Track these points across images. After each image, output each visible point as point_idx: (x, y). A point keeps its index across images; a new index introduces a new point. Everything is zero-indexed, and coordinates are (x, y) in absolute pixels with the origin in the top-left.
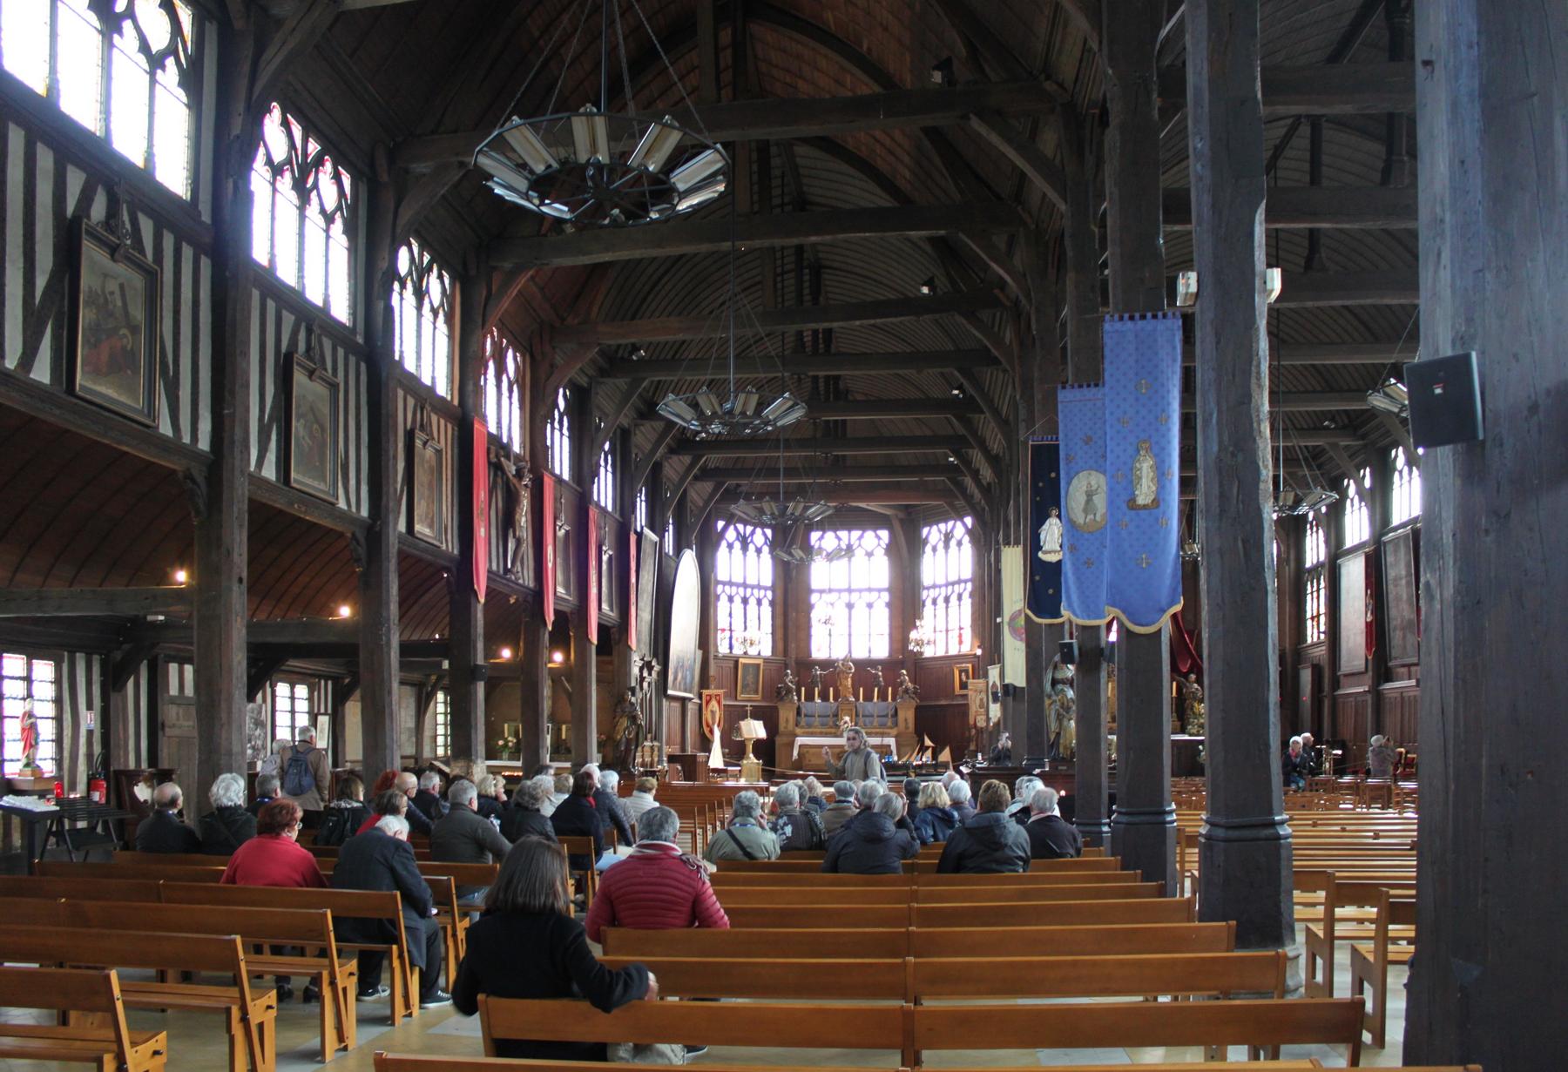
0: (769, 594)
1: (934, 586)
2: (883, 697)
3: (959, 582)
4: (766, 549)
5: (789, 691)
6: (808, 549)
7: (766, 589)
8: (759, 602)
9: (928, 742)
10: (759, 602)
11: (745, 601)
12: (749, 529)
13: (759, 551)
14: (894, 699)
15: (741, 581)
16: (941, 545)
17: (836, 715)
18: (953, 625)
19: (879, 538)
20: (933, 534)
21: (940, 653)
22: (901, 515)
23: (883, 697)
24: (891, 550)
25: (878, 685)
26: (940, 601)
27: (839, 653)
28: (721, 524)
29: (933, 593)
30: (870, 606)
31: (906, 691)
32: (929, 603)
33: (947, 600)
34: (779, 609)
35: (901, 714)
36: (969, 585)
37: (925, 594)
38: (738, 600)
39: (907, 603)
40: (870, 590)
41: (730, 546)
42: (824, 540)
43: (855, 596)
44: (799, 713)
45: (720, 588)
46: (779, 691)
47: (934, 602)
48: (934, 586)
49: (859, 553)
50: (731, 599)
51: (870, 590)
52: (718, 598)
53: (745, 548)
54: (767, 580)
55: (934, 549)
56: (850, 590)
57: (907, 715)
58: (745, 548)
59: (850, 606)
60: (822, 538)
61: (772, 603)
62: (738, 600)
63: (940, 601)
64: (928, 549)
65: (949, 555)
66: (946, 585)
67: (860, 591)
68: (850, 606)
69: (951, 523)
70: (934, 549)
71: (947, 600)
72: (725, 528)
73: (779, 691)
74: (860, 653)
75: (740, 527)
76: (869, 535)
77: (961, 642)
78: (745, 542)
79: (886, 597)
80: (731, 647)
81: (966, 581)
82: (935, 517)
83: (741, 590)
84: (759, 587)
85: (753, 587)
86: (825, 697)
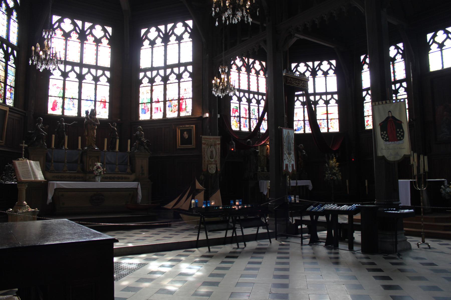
2: (123, 148)
3: (179, 65)
9: (198, 186)
17: (82, 161)
19: (105, 31)
21: (158, 116)
23: (123, 148)
26: (158, 80)
27: (71, 112)
29: (149, 74)
30: (96, 79)
31: (141, 143)
32: (145, 81)
36: (190, 68)
37: (142, 75)
39: (125, 79)
40: (97, 67)
47: (152, 81)
48: (152, 69)
49: (90, 39)
55: (152, 43)
56: (81, 65)
57: (142, 163)
59: (81, 77)
60: (60, 21)
63: (158, 80)
64: (146, 43)
68: (81, 77)
69: (170, 26)
70: (152, 43)
71: (165, 79)
77: (180, 109)
79: (108, 74)
81: (186, 65)
86: (73, 145)
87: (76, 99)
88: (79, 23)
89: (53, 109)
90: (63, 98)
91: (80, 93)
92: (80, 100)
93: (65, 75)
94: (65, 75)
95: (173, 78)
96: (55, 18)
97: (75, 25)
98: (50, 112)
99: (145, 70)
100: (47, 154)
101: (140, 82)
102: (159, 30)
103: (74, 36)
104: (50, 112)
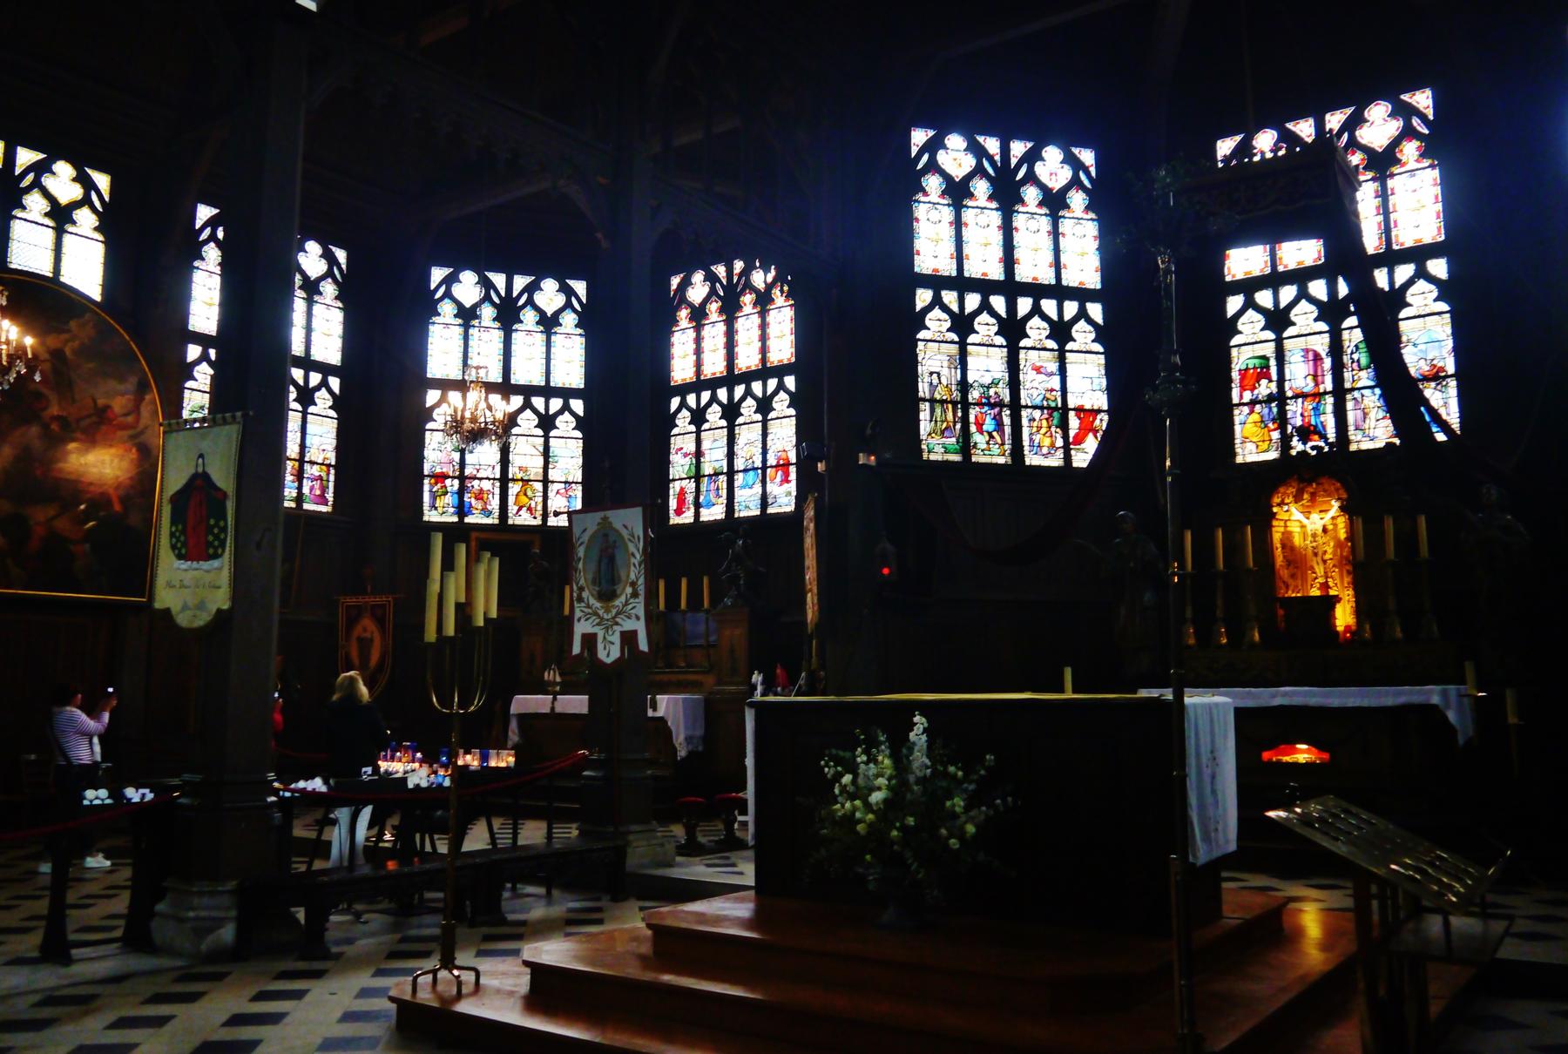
0: (1095, 311)
8: (1061, 332)
10: (1061, 332)
11: (1012, 330)
12: (1018, 148)
28: (919, 137)
38: (985, 327)
41: (957, 192)
45: (923, 297)
50: (962, 325)
52: (918, 321)
61: (1102, 334)
62: (985, 327)
72: (933, 146)
75: (992, 145)
80: (966, 446)
83: (998, 303)
84: (1060, 292)
85: (1037, 291)
87: (1326, 393)
92: (1340, 393)
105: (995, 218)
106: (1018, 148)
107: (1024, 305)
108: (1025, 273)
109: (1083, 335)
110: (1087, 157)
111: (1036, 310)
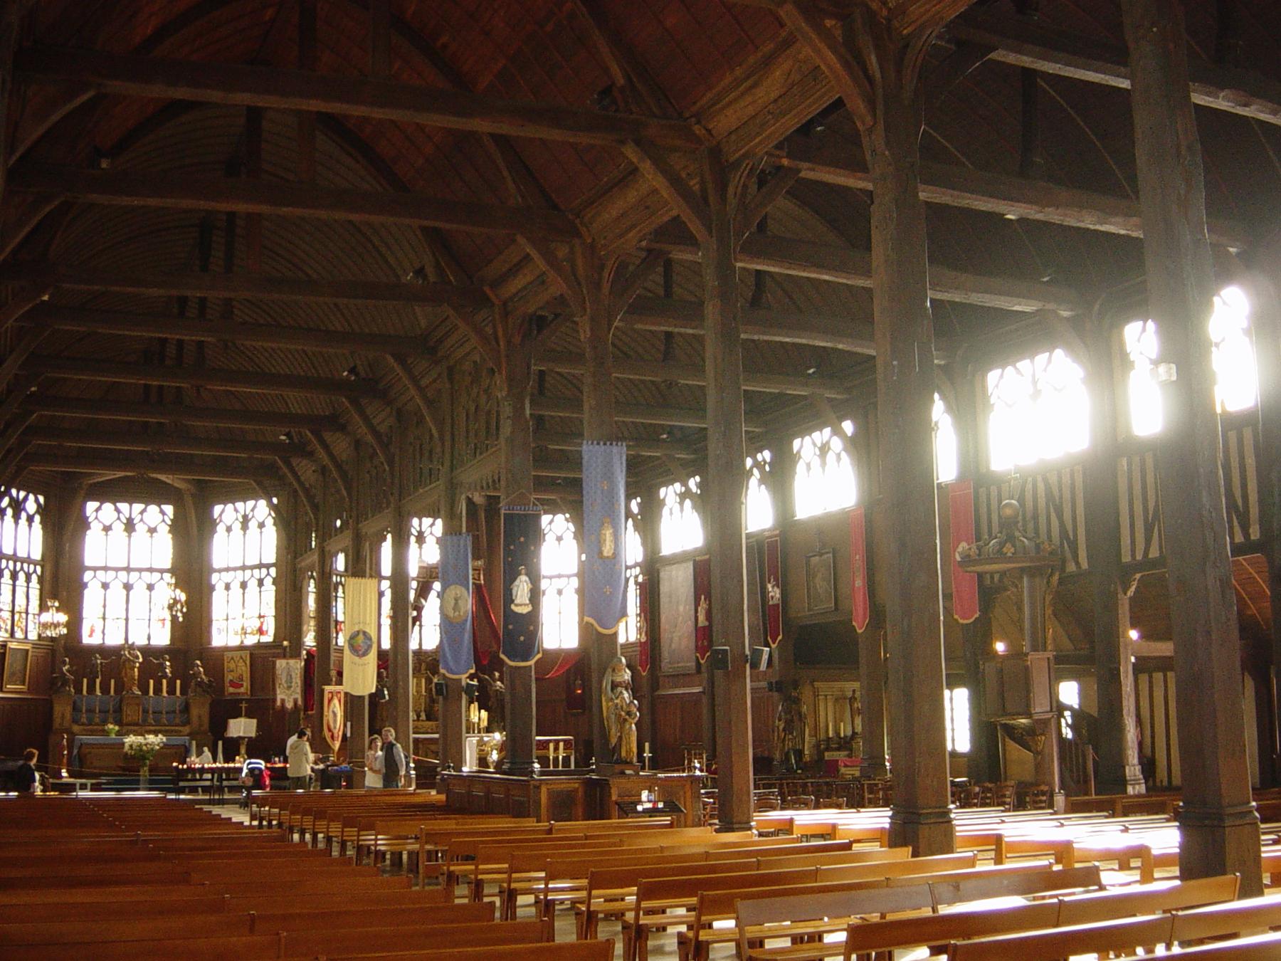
0: (39, 569)
1: (228, 569)
3: (260, 566)
4: (37, 518)
5: (65, 682)
6: (84, 524)
7: (35, 563)
8: (28, 579)
10: (28, 579)
11: (14, 576)
12: (22, 494)
13: (30, 519)
14: (184, 691)
15: (11, 552)
16: (237, 527)
18: (252, 610)
20: (226, 513)
22: (193, 490)
24: (178, 528)
25: (165, 676)
27: (114, 639)
29: (227, 577)
30: (150, 587)
31: (200, 684)
32: (219, 588)
33: (244, 585)
34: (47, 586)
35: (195, 712)
36: (273, 571)
37: (215, 578)
40: (151, 570)
42: (100, 513)
43: (134, 575)
44: (76, 708)
46: (53, 682)
47: (227, 587)
51: (151, 570)
53: (16, 517)
54: (37, 555)
55: (229, 529)
58: (16, 517)
59: (128, 587)
60: (97, 510)
61: (41, 580)
63: (236, 587)
64: (221, 529)
65: (246, 535)
66: (244, 568)
67: (140, 570)
68: (128, 587)
70: (229, 529)
71: (244, 585)
73: (53, 682)
74: (139, 639)
75: (14, 492)
76: (153, 509)
78: (17, 506)
81: (268, 566)
82: (231, 495)
83: (11, 563)
84: (29, 560)
88: (124, 506)
89: (91, 636)
90: (104, 619)
91: (127, 610)
92: (127, 619)
93: (105, 586)
94: (105, 586)
95: (253, 584)
96: (91, 506)
97: (117, 510)
98: (86, 640)
99: (220, 571)
100: (74, 703)
101: (212, 588)
102: (236, 510)
103: (119, 528)
104: (86, 640)
105: (13, 525)
106: (22, 494)
107: (19, 564)
108: (20, 554)
109: (34, 578)
110: (41, 499)
111: (22, 569)
